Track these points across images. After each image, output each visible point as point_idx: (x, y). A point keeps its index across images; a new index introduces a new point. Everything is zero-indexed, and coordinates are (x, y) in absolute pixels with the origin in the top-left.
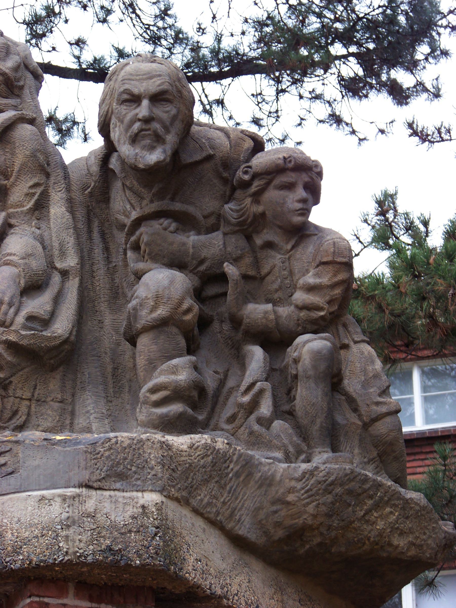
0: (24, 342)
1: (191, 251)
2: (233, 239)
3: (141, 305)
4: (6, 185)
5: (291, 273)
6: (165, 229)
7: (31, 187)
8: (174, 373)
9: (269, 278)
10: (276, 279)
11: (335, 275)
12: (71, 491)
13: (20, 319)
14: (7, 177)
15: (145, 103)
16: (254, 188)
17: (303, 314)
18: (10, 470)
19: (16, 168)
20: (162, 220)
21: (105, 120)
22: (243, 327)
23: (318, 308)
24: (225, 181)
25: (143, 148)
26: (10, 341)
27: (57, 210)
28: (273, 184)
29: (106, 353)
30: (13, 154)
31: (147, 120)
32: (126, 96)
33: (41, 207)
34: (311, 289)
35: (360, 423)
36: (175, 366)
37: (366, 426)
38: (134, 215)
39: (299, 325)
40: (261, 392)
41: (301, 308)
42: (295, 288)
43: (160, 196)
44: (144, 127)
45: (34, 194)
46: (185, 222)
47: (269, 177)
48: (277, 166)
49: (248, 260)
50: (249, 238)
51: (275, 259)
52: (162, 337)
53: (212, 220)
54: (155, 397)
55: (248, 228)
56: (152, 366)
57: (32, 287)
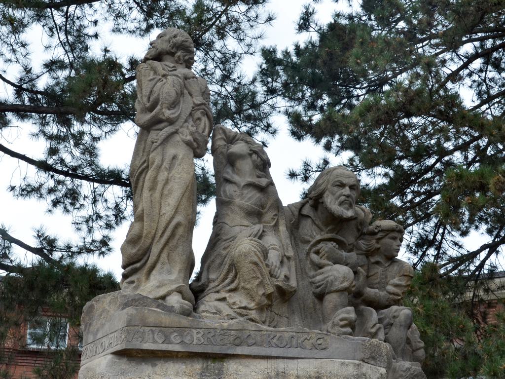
0: (284, 287)
1: (344, 259)
2: (361, 257)
3: (336, 280)
4: (262, 212)
5: (386, 277)
6: (334, 247)
7: (274, 215)
8: (348, 313)
9: (372, 277)
10: (377, 278)
11: (407, 282)
12: (357, 362)
13: (282, 277)
14: (263, 207)
15: (347, 188)
16: (379, 236)
17: (391, 296)
18: (324, 347)
19: (268, 205)
20: (332, 242)
21: (322, 192)
22: (363, 298)
23: (398, 295)
24: (358, 230)
25: (345, 208)
26: (279, 285)
27: (282, 228)
28: (388, 236)
29: (300, 299)
30: (268, 198)
31: (348, 196)
32: (338, 183)
33: (276, 225)
34: (396, 286)
35: (411, 350)
36: (349, 310)
37: (414, 351)
38: (318, 237)
39: (387, 301)
40: (379, 328)
41: (390, 293)
42: (387, 284)
43: (331, 231)
44: (347, 199)
45: (274, 219)
46: (341, 244)
47: (388, 233)
48: (393, 228)
49: (366, 268)
50: (367, 257)
51: (379, 270)
52: (343, 296)
53: (351, 247)
54: (342, 323)
55: (368, 254)
56: (336, 308)
57: (282, 262)
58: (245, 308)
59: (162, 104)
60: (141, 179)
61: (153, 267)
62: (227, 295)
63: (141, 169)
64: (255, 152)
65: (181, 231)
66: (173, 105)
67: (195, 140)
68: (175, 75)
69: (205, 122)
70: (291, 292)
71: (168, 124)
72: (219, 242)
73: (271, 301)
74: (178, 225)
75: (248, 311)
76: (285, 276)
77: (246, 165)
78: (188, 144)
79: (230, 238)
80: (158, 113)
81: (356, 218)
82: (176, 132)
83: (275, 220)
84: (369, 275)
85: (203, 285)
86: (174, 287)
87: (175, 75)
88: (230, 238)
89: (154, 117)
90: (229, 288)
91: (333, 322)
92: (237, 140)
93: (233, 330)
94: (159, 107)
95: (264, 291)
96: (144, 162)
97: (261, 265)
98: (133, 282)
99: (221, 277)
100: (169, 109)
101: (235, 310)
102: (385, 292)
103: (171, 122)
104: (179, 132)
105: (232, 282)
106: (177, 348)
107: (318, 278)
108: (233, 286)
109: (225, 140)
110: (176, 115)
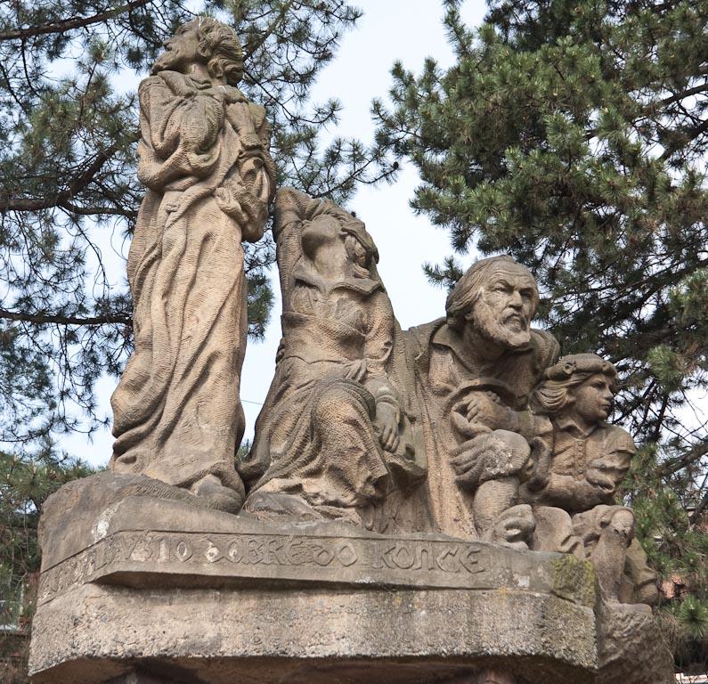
4: (364, 337)
7: (386, 344)
15: (517, 293)
19: (376, 326)
20: (490, 393)
23: (608, 486)
24: (535, 372)
34: (604, 469)
38: (465, 384)
43: (487, 373)
44: (515, 312)
45: (387, 350)
47: (589, 375)
58: (336, 503)
59: (186, 143)
60: (149, 278)
61: (168, 433)
62: (304, 481)
63: (148, 259)
64: (352, 233)
65: (218, 367)
66: (206, 146)
67: (245, 208)
68: (209, 95)
69: (261, 178)
70: (419, 478)
71: (197, 179)
72: (288, 391)
73: (383, 492)
74: (212, 359)
75: (341, 509)
76: (407, 449)
77: (335, 255)
78: (232, 215)
79: (308, 383)
80: (178, 159)
81: (530, 351)
82: (210, 195)
83: (388, 353)
84: (556, 452)
85: (260, 464)
86: (207, 466)
87: (209, 95)
88: (308, 383)
89: (172, 166)
90: (307, 468)
91: (495, 531)
92: (320, 213)
93: (317, 537)
94: (179, 150)
95: (369, 473)
96: (153, 248)
97: (361, 422)
98: (133, 459)
99: (292, 450)
100: (198, 154)
101: (320, 507)
102: (584, 481)
103: (202, 175)
104: (215, 194)
105: (312, 458)
106: (210, 570)
107: (467, 455)
108: (313, 465)
109: (297, 213)
110: (210, 163)
